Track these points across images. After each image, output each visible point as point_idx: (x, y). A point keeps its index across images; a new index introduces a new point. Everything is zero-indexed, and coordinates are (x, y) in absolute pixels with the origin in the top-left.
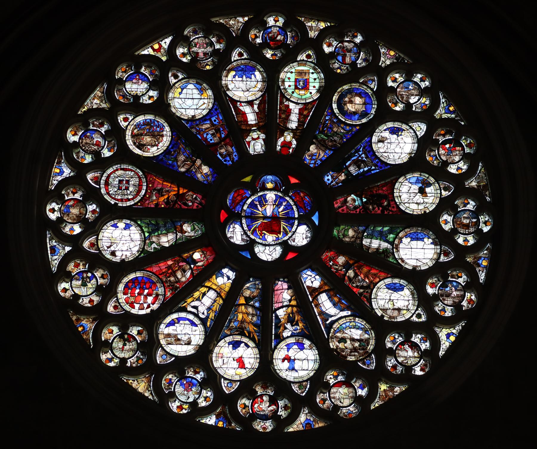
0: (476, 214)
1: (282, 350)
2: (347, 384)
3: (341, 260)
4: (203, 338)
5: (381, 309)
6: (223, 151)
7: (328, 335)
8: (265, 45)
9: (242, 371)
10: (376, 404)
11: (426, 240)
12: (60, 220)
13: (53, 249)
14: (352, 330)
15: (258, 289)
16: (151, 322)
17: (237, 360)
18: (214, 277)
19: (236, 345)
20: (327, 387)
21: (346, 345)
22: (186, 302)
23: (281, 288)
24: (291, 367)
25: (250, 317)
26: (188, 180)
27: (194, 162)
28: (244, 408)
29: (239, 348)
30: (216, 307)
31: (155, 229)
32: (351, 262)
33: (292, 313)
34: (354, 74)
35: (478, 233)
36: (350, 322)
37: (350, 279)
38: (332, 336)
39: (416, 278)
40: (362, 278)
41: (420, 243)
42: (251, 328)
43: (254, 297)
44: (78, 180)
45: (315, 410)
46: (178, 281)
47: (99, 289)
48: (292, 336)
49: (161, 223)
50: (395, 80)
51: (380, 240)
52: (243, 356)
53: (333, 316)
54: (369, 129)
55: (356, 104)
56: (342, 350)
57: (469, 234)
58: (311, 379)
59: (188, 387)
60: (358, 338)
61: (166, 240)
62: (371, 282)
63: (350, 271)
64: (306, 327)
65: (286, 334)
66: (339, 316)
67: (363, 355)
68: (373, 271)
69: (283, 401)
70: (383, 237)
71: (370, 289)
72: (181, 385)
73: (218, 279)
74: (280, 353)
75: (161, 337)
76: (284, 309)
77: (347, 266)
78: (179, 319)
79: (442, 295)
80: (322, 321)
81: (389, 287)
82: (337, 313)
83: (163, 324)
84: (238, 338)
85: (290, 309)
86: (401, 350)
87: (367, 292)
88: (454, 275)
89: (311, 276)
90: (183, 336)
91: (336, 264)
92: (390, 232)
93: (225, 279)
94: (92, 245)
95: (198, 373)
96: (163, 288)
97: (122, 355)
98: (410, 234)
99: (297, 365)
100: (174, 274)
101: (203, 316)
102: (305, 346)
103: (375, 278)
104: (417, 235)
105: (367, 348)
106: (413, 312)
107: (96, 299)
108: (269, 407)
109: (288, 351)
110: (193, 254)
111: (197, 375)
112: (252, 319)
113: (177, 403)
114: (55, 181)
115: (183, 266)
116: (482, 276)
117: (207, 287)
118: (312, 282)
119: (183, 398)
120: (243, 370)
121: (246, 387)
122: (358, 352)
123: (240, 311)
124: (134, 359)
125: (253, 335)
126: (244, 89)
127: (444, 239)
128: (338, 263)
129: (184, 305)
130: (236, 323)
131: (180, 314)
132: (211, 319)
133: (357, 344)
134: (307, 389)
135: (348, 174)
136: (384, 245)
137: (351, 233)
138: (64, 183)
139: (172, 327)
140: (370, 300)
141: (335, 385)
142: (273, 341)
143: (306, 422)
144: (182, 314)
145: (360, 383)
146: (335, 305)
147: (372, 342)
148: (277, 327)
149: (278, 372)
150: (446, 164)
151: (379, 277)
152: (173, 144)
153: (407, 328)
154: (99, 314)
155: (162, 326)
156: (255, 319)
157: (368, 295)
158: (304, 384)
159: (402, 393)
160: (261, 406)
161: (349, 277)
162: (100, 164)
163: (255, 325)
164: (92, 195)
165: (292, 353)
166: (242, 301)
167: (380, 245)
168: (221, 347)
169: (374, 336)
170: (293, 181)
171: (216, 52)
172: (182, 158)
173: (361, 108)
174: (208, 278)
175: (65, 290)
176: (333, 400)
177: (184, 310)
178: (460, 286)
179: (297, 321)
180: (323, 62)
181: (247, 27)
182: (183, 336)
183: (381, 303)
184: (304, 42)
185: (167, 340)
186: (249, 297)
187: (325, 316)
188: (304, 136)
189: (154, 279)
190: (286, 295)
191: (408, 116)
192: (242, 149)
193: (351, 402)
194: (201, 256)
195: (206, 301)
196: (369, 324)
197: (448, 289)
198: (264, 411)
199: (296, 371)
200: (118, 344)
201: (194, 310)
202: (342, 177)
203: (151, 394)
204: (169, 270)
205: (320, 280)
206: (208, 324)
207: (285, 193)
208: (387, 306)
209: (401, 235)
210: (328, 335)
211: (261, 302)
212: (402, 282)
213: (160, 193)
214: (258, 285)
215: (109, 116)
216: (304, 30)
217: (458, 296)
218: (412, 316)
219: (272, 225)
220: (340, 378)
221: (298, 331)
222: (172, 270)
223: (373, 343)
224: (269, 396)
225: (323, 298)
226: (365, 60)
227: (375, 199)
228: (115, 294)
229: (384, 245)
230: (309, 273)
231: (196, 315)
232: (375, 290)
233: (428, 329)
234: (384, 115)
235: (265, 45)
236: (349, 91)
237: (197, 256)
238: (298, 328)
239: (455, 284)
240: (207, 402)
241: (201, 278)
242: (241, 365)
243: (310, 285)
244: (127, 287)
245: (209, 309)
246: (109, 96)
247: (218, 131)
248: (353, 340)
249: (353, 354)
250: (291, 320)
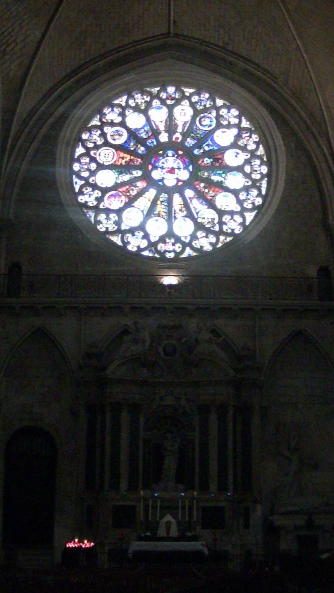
0: (260, 166)
2: (207, 237)
6: (150, 141)
8: (167, 98)
10: (220, 245)
12: (80, 171)
13: (76, 183)
16: (119, 212)
26: (134, 153)
27: (137, 146)
31: (121, 173)
32: (207, 186)
34: (206, 110)
35: (261, 173)
37: (206, 193)
39: (235, 193)
44: (87, 154)
45: (193, 248)
46: (131, 195)
47: (97, 199)
49: (123, 171)
50: (223, 112)
54: (212, 132)
55: (206, 122)
61: (126, 177)
68: (216, 190)
70: (220, 175)
77: (205, 187)
91: (200, 187)
92: (223, 173)
93: (152, 193)
94: (93, 181)
97: (106, 226)
100: (129, 192)
107: (95, 203)
114: (77, 155)
116: (264, 192)
121: (162, 239)
124: (112, 228)
126: (159, 115)
127: (247, 176)
135: (204, 150)
137: (206, 174)
138: (82, 155)
140: (215, 201)
148: (175, 214)
150: (246, 145)
152: (129, 138)
153: (232, 213)
154: (96, 209)
159: (230, 241)
162: (97, 147)
163: (165, 213)
164: (93, 160)
170: (180, 152)
171: (146, 102)
172: (132, 144)
173: (209, 123)
175: (81, 200)
177: (133, 206)
180: (193, 105)
181: (159, 92)
184: (184, 97)
188: (185, 135)
189: (121, 194)
191: (229, 126)
192: (158, 141)
195: (144, 203)
200: (104, 222)
202: (202, 151)
207: (177, 158)
211: (168, 203)
213: (123, 158)
215: (101, 128)
216: (183, 92)
219: (172, 171)
225: (195, 201)
226: (210, 104)
227: (216, 160)
228: (103, 201)
233: (241, 213)
234: (219, 126)
235: (167, 98)
236: (204, 117)
241: (140, 194)
244: (109, 197)
246: (100, 120)
247: (147, 133)
250: (181, 210)
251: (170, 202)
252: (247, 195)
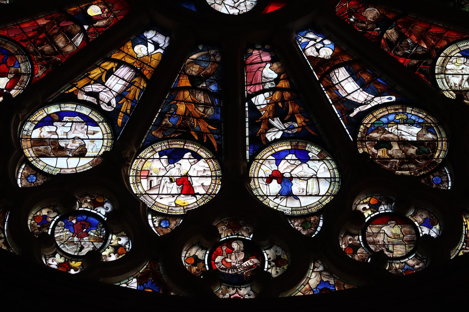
1: (266, 163)
2: (397, 217)
3: (371, 13)
4: (110, 144)
5: (454, 91)
7: (355, 136)
9: (190, 201)
14: (402, 127)
15: (215, 62)
17: (177, 181)
18: (129, 44)
19: (174, 156)
20: (359, 223)
21: (390, 152)
22: (75, 86)
23: (259, 60)
24: (286, 191)
25: (201, 109)
28: (194, 265)
29: (181, 161)
30: (135, 93)
32: (391, 16)
33: (282, 99)
36: (397, 114)
38: (362, 137)
40: (413, 42)
42: (203, 126)
43: (207, 76)
46: (60, 51)
48: (284, 139)
52: (190, 174)
53: (361, 104)
56: (384, 161)
58: (324, 211)
59: (80, 231)
60: (415, 139)
63: (389, 31)
64: (309, 124)
65: (270, 136)
66: (373, 104)
67: (425, 169)
69: (272, 250)
72: (67, 226)
73: (137, 48)
74: (263, 168)
75: (25, 144)
76: (267, 94)
77: (383, 23)
78: (60, 116)
80: (341, 113)
82: (369, 98)
83: (29, 124)
84: (178, 145)
85: (277, 96)
87: (426, 64)
89: (315, 40)
90: (70, 141)
95: (102, 205)
96: (28, 63)
99: (297, 186)
100: (51, 41)
101: (109, 109)
102: (310, 155)
103: (437, 42)
105: (433, 156)
108: (244, 260)
109: (277, 164)
110: (87, 7)
111: (99, 209)
112: (204, 112)
113: (59, 259)
115: (68, 26)
117: (115, 61)
118: (318, 50)
119: (70, 250)
120: (190, 197)
122: (416, 164)
123: (181, 98)
125: (208, 139)
128: (366, 18)
129: (70, 91)
130: (173, 120)
131: (62, 105)
132: (125, 113)
133: (412, 151)
134: (319, 229)
139: (47, 129)
141: (373, 221)
142: (248, 148)
143: (320, 287)
144: (68, 105)
145: (425, 216)
146: (364, 86)
147: (442, 146)
148: (254, 125)
149: (261, 199)
151: (446, 39)
155: (28, 126)
156: (210, 111)
158: (312, 219)
160: (228, 260)
161: (387, 40)
163: (210, 121)
165: (284, 167)
166: (185, 82)
168: (146, 159)
169: (444, 135)
174: (119, 46)
176: (372, 247)
177: (73, 99)
179: (293, 114)
182: (70, 141)
183: (455, 80)
185: (37, 150)
186: (198, 76)
187: (347, 105)
190: (269, 73)
193: (409, 250)
194: (102, 10)
196: (432, 116)
198: (235, 267)
199: (296, 197)
201: (89, 99)
203: (5, 243)
204: (40, 33)
205: (333, 47)
206: (120, 121)
210: (355, 136)
214: (214, 55)
220: (383, 209)
221: (295, 131)
222: (46, 33)
223: (445, 148)
224: (244, 241)
225: (341, 74)
230: (311, 36)
231: (96, 108)
232: (440, 60)
237: (94, 11)
238: (296, 125)
240: (119, 255)
242: (186, 188)
243: (315, 54)
245: (120, 96)
248: (403, 143)
249: (406, 166)
251: (231, 85)
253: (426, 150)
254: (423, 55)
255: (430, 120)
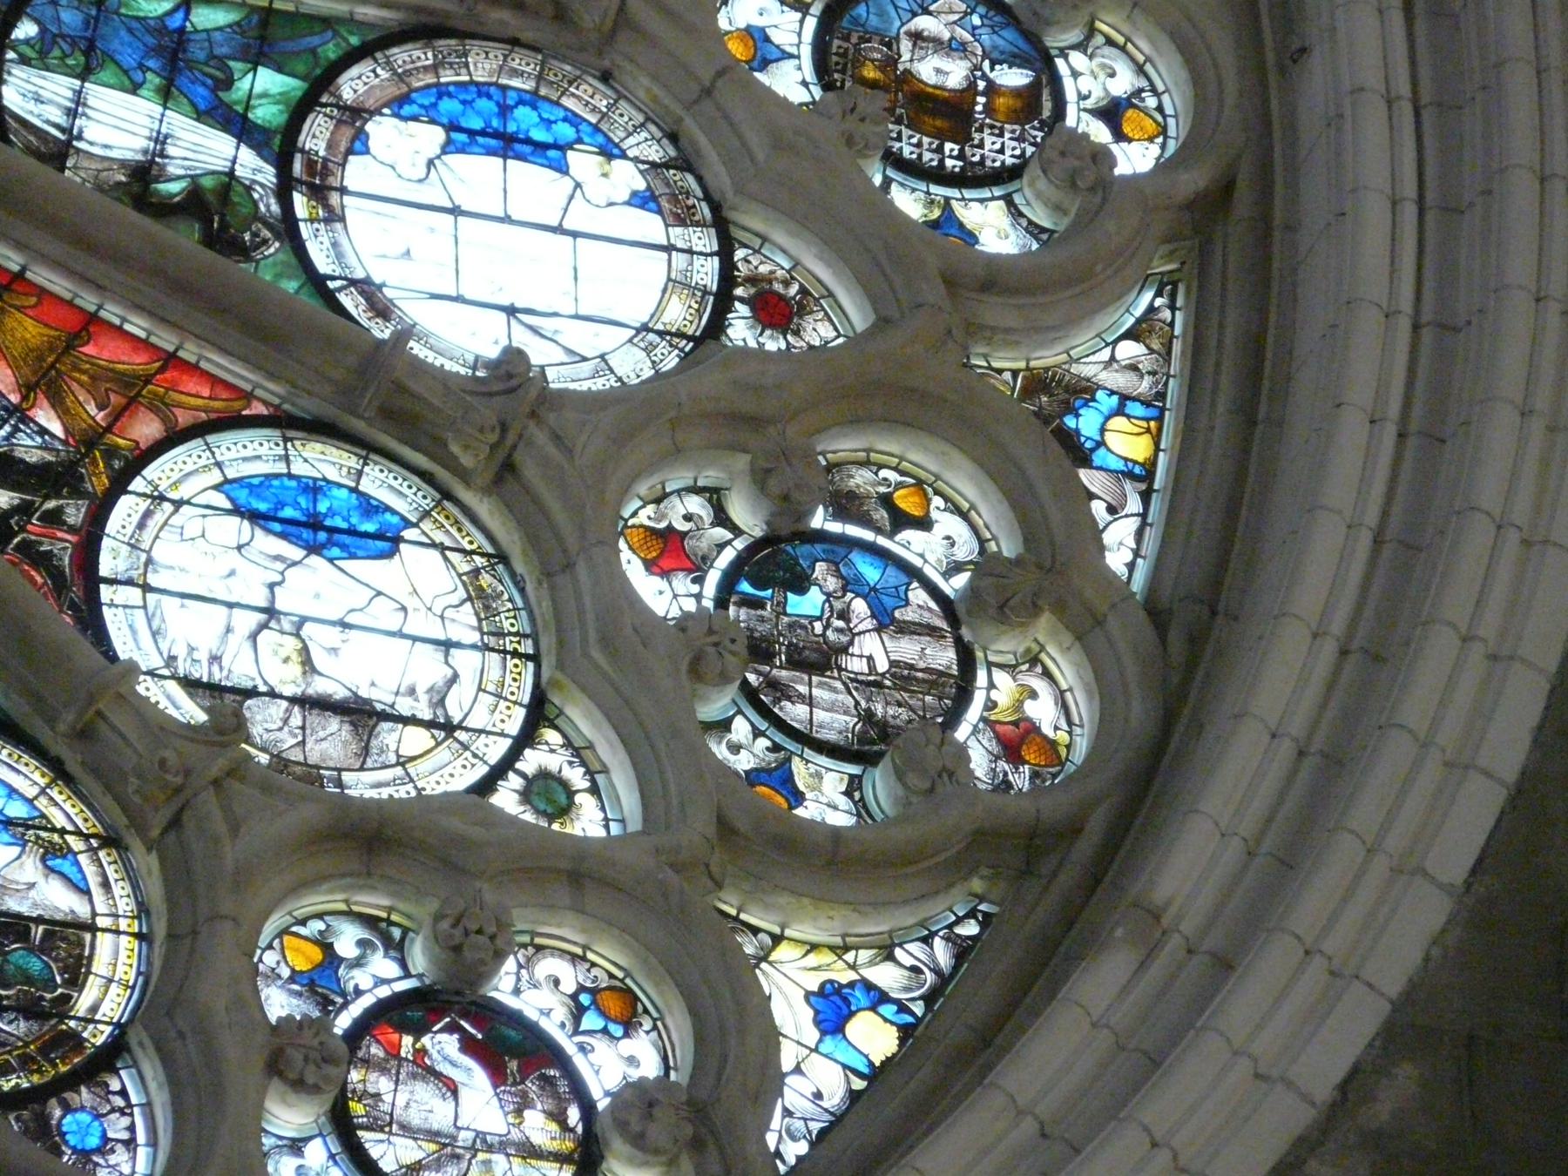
11: (583, 162)
41: (531, 186)
51: (166, 95)
57: (973, 178)
62: (89, 440)
71: (77, 493)
79: (760, 651)
81: (256, 507)
86: (391, 1062)
88: (852, 496)
98: (442, 91)
104: (505, 111)
106: (496, 750)
136: (201, 149)
140: (81, 588)
151: (160, 408)
157: (62, 548)
167: (161, 139)
178: (918, 596)
197: (806, 604)
208: (239, 670)
209: (353, 84)
212: (379, 482)
217: (903, 676)
218: (486, 786)
223: (127, 970)
229: (201, 149)
232: (125, 511)
239: (870, 572)
252: (774, 562)
253: (35, 965)
254: (42, 469)
255: (64, 810)
